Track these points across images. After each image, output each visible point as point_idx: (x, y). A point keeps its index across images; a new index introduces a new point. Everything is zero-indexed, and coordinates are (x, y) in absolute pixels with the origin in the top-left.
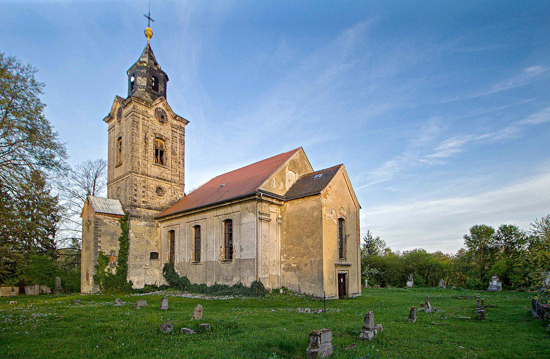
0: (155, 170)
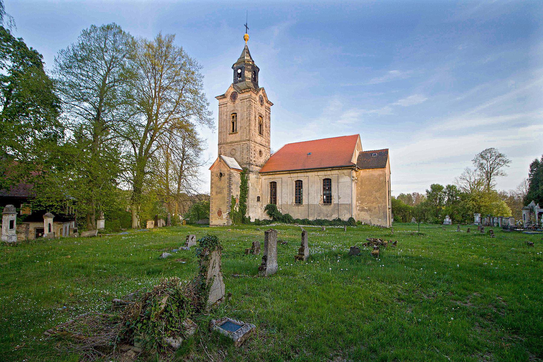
0: (258, 139)
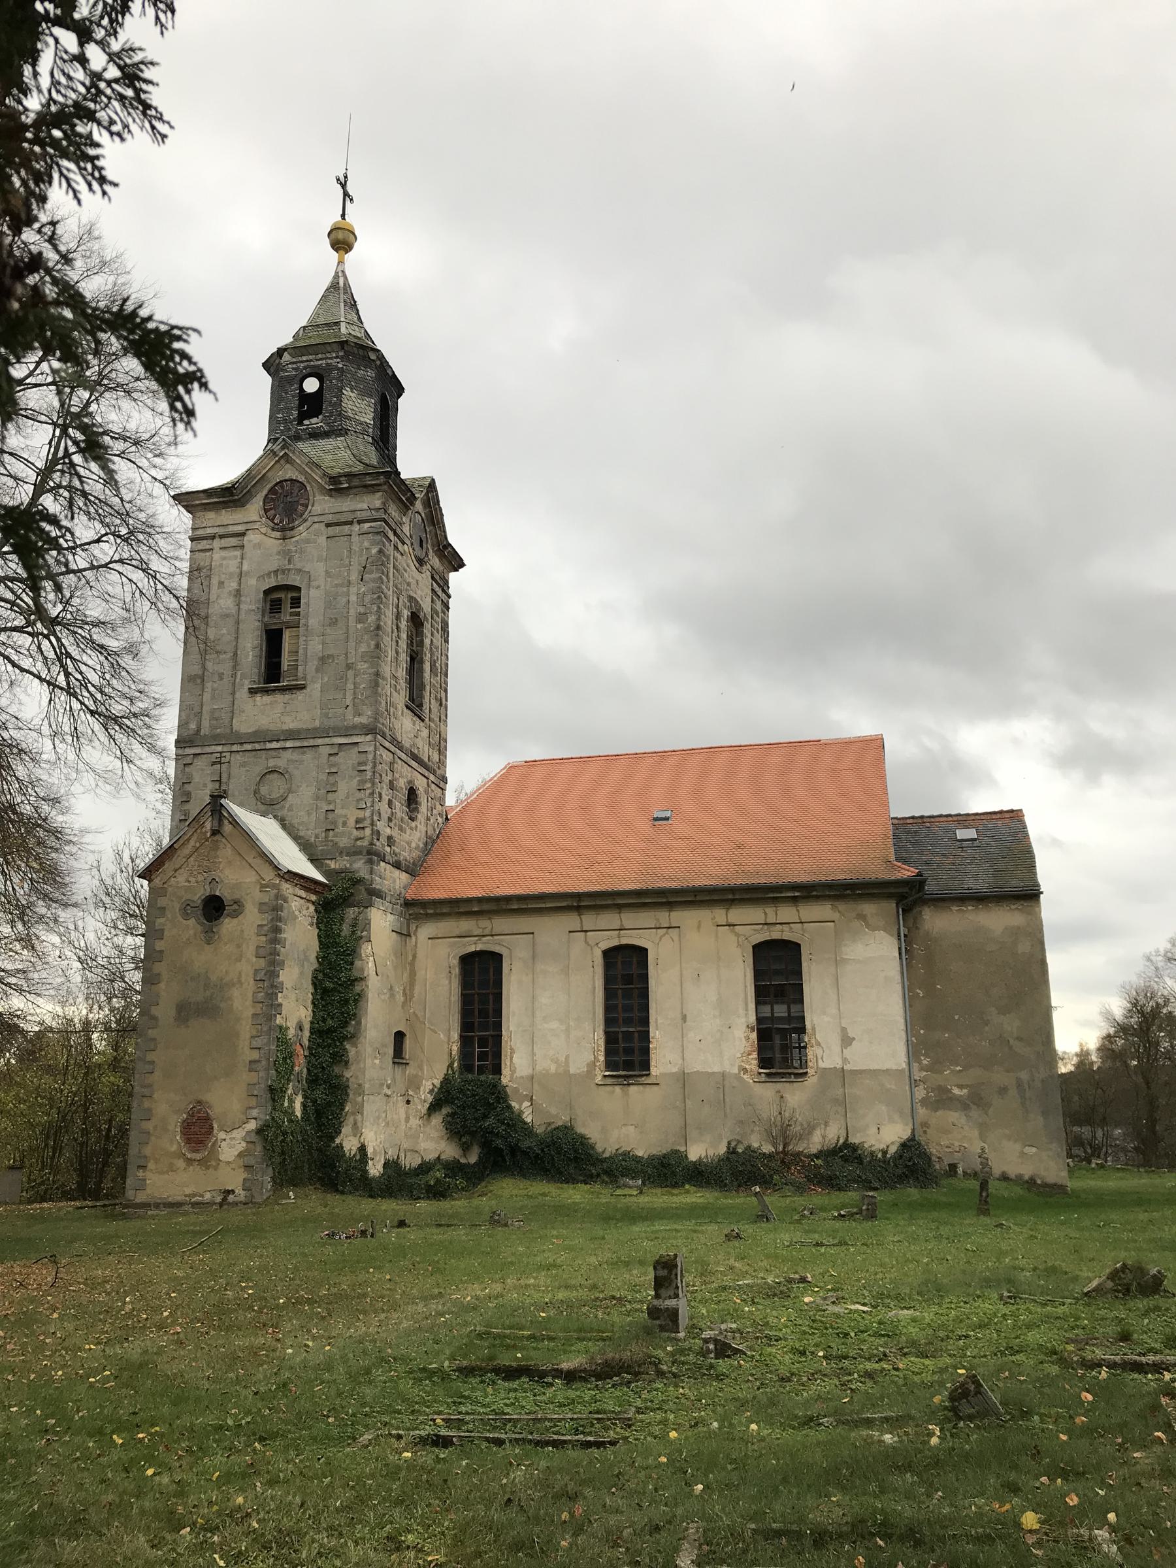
0: (405, 726)
